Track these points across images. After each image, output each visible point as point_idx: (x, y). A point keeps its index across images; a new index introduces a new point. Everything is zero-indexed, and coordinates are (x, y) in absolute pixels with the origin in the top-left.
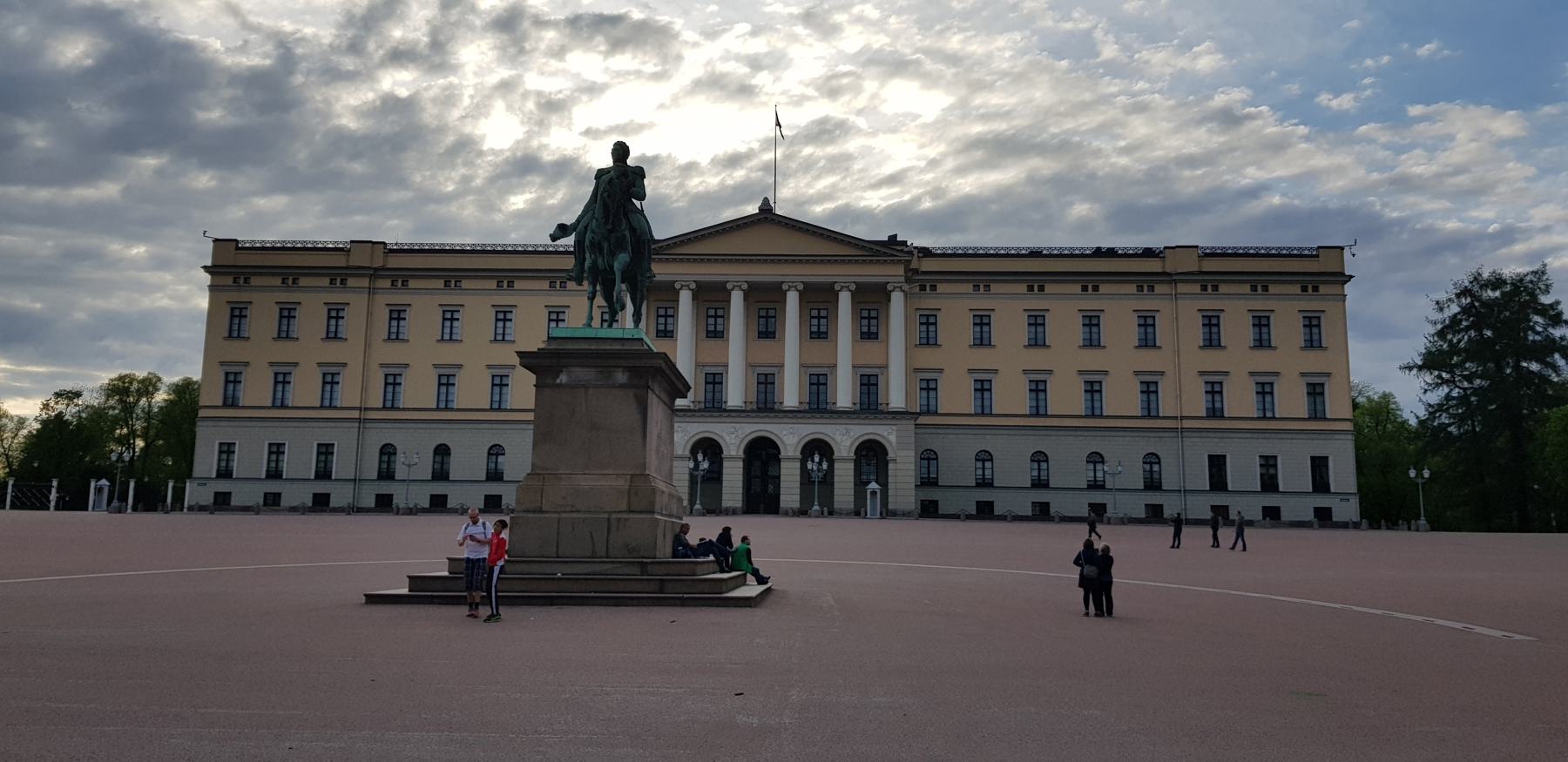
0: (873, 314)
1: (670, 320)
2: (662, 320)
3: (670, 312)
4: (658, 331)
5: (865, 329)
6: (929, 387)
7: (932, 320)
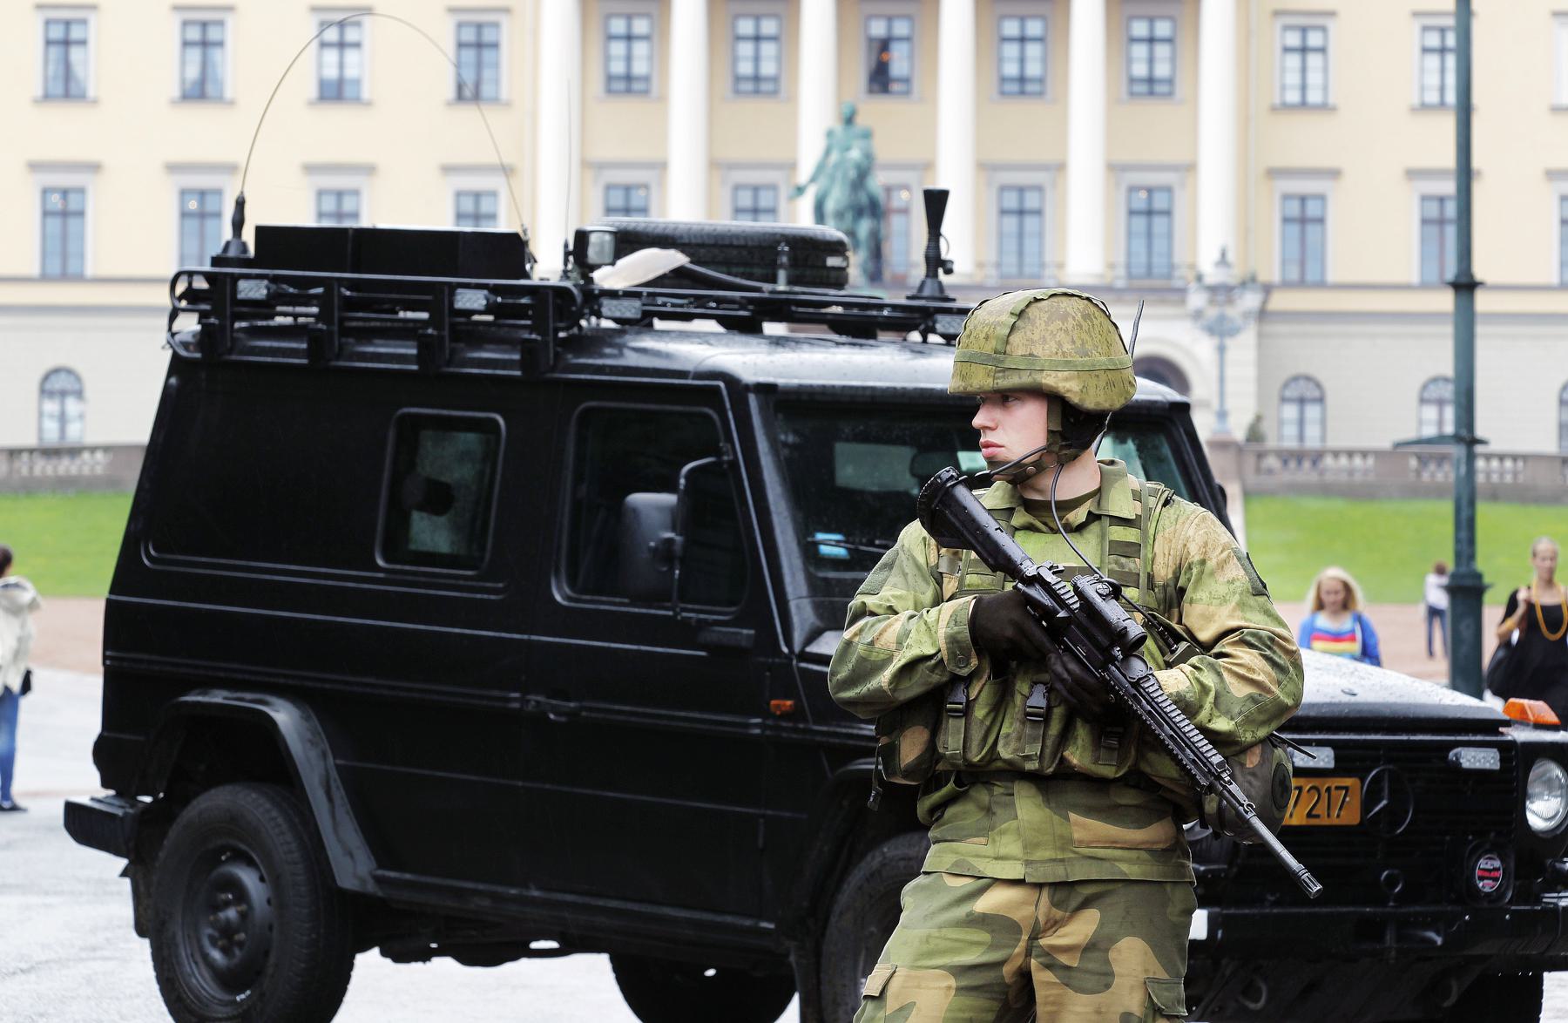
0: (1163, 29)
1: (640, 49)
2: (618, 48)
3: (640, 26)
4: (610, 78)
5: (1140, 70)
6: (1304, 219)
7: (1314, 39)
